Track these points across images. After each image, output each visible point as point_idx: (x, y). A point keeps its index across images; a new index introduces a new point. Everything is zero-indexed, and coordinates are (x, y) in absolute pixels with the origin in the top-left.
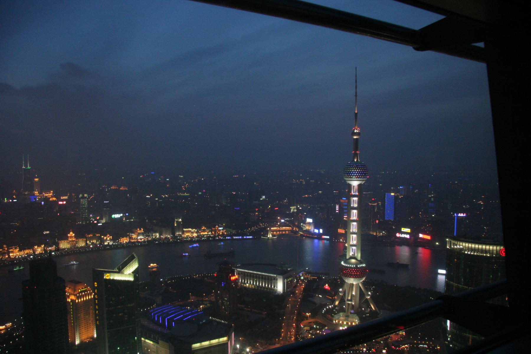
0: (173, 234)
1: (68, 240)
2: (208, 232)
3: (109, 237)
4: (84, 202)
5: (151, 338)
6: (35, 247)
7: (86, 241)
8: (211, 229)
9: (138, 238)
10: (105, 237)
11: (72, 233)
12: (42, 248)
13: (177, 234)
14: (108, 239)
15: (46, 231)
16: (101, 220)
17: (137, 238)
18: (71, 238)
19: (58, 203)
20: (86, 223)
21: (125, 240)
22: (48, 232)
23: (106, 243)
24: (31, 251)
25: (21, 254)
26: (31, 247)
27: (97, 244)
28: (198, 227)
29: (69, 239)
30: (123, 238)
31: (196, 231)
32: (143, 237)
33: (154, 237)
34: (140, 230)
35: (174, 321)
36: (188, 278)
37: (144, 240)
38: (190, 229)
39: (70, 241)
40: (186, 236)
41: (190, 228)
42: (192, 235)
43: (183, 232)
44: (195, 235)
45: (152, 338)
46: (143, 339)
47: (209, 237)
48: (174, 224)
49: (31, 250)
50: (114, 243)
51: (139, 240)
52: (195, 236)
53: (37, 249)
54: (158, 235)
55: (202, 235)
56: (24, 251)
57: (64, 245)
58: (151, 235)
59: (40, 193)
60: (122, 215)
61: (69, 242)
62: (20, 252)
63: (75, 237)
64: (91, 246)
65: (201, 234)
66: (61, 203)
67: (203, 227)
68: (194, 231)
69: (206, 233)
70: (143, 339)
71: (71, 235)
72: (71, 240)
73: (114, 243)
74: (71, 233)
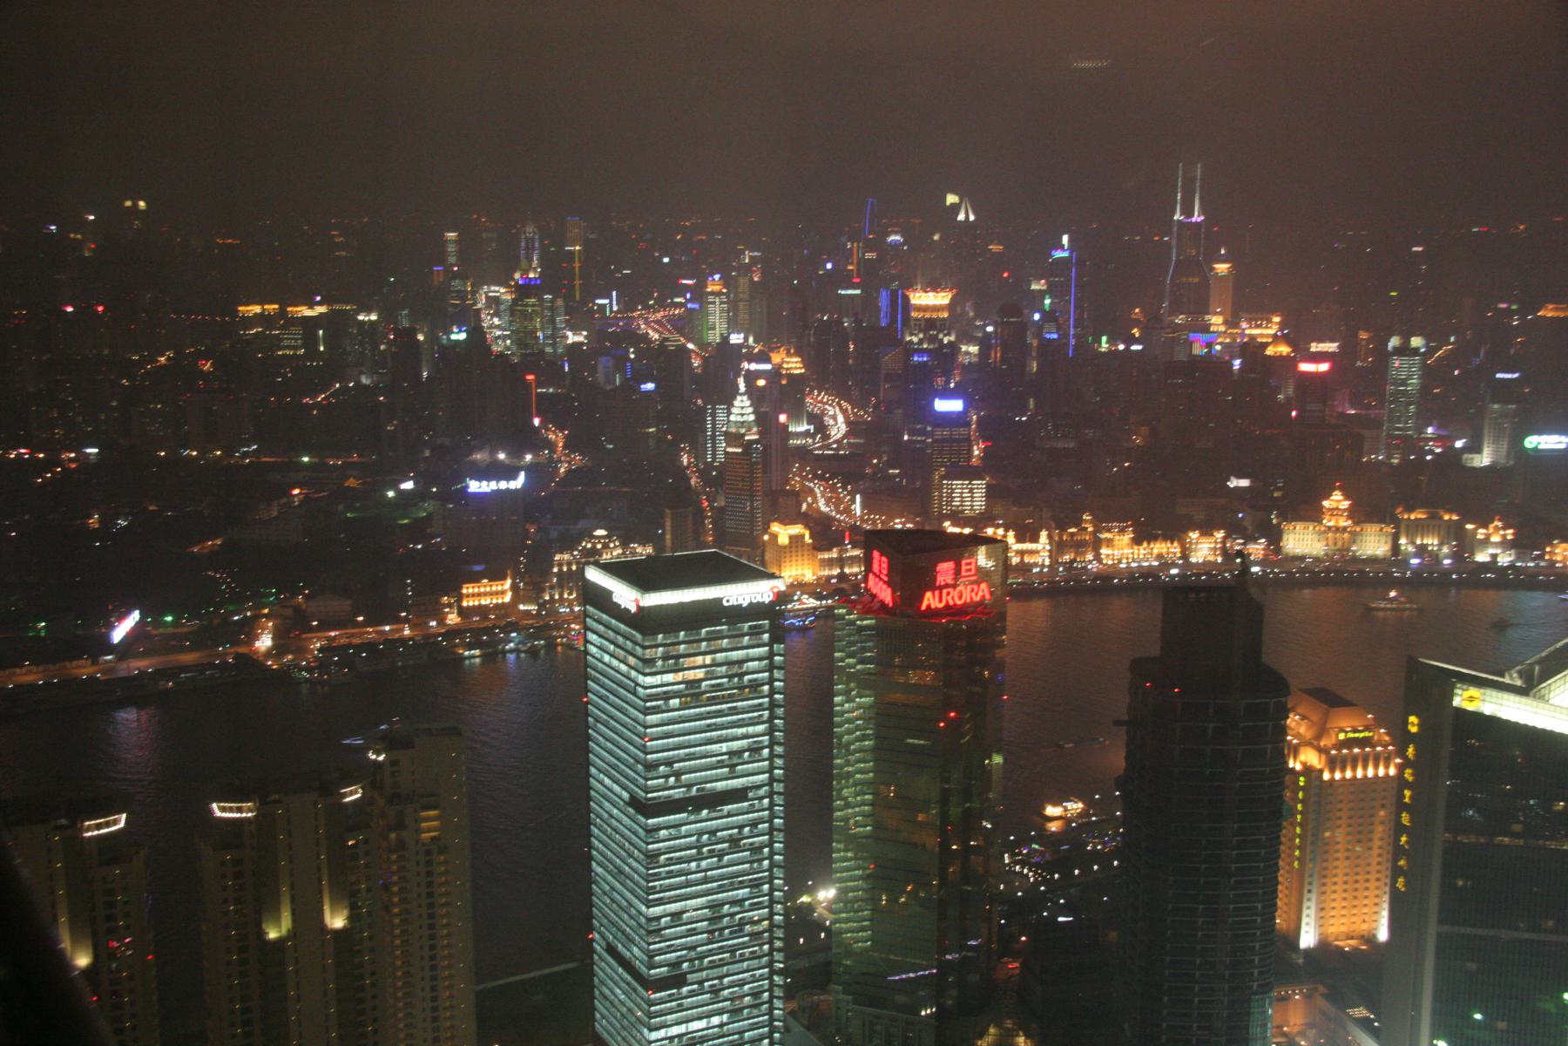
1: (1320, 522)
3: (1502, 532)
4: (1407, 374)
6: (1191, 534)
7: (1396, 537)
10: (1481, 531)
11: (1341, 498)
14: (1495, 539)
15: (1239, 477)
16: (1471, 453)
18: (1332, 515)
19: (1296, 366)
20: (1404, 460)
22: (1245, 483)
23: (1482, 557)
24: (1174, 549)
25: (1139, 555)
26: (1174, 530)
27: (1441, 555)
29: (1324, 521)
49: (1176, 544)
53: (1197, 543)
56: (1149, 544)
57: (1302, 541)
59: (1231, 322)
61: (1325, 532)
62: (1136, 547)
63: (1352, 513)
64: (1415, 561)
66: (1305, 367)
71: (1335, 505)
72: (1331, 524)
73: (1518, 558)
74: (1337, 496)
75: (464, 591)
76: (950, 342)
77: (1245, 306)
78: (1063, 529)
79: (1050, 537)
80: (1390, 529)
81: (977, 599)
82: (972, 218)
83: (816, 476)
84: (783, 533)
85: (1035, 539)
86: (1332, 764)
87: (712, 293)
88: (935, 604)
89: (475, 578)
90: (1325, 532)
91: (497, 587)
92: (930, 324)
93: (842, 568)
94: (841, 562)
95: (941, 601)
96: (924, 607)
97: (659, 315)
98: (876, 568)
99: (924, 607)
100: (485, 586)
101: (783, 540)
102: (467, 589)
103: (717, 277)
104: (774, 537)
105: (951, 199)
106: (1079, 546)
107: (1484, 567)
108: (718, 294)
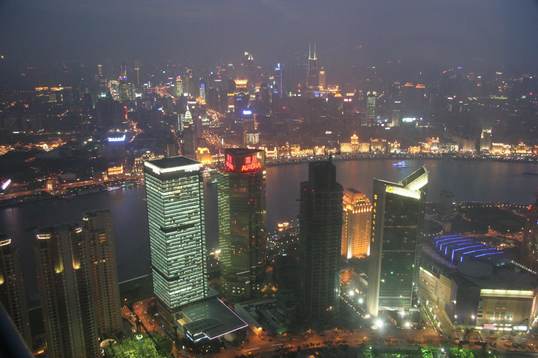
0: (478, 147)
1: (350, 143)
2: (527, 151)
4: (372, 101)
5: (431, 270)
6: (316, 147)
7: (370, 147)
8: (533, 146)
9: (432, 149)
10: (392, 144)
12: (323, 149)
13: (483, 148)
14: (396, 146)
15: (328, 131)
17: (431, 148)
20: (372, 125)
21: (415, 150)
22: (330, 132)
23: (392, 151)
24: (312, 151)
26: (311, 147)
28: (513, 142)
30: (413, 148)
31: (510, 147)
32: (438, 149)
33: (451, 149)
34: (435, 139)
35: (463, 256)
36: (489, 206)
37: (439, 152)
38: (502, 144)
39: (353, 144)
40: (495, 153)
41: (501, 143)
42: (503, 152)
43: (491, 147)
44: (508, 152)
45: (433, 269)
46: (421, 268)
47: (527, 158)
48: (480, 136)
49: (312, 150)
50: (401, 151)
51: (432, 152)
52: (508, 154)
53: (318, 150)
54: (457, 147)
55: (518, 153)
57: (346, 148)
58: (448, 147)
59: (325, 88)
60: (414, 119)
61: (352, 146)
64: (375, 153)
65: (517, 152)
66: (346, 100)
67: (520, 144)
68: (508, 147)
69: (524, 152)
70: (421, 268)
71: (354, 138)
72: (353, 143)
73: (401, 151)
74: (355, 135)
75: (109, 170)
76: (247, 94)
77: (329, 83)
78: (281, 147)
79: (277, 149)
80: (369, 144)
81: (257, 167)
82: (252, 59)
83: (210, 134)
84: (201, 150)
85: (273, 150)
86: (355, 209)
87: (178, 82)
88: (246, 169)
89: (112, 166)
90: (352, 146)
91: (118, 169)
92: (242, 89)
93: (219, 160)
94: (218, 158)
95: (247, 168)
96: (242, 170)
97: (163, 88)
98: (228, 159)
99: (242, 170)
100: (115, 168)
101: (202, 152)
102: (110, 170)
103: (179, 77)
104: (199, 151)
105: (246, 53)
106: (285, 151)
107: (393, 154)
108: (180, 82)
